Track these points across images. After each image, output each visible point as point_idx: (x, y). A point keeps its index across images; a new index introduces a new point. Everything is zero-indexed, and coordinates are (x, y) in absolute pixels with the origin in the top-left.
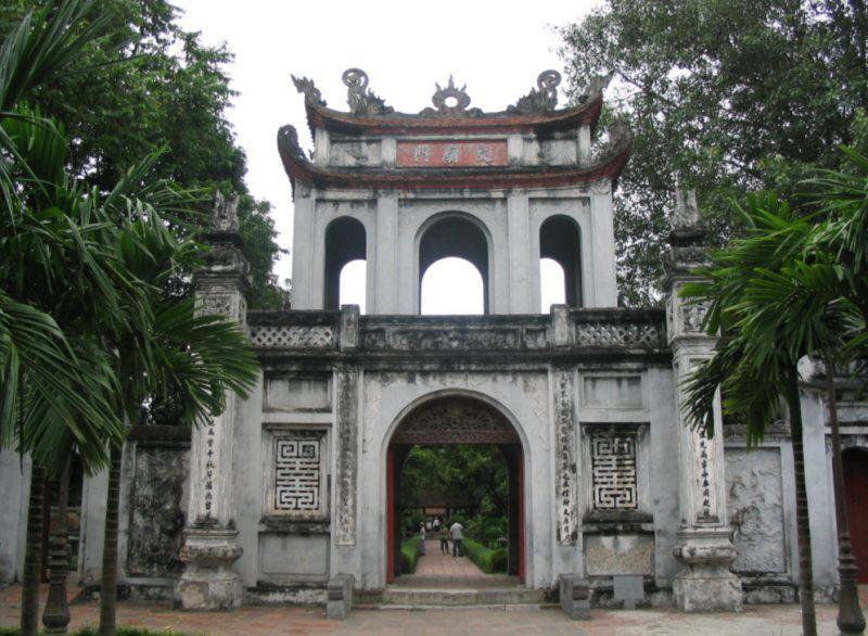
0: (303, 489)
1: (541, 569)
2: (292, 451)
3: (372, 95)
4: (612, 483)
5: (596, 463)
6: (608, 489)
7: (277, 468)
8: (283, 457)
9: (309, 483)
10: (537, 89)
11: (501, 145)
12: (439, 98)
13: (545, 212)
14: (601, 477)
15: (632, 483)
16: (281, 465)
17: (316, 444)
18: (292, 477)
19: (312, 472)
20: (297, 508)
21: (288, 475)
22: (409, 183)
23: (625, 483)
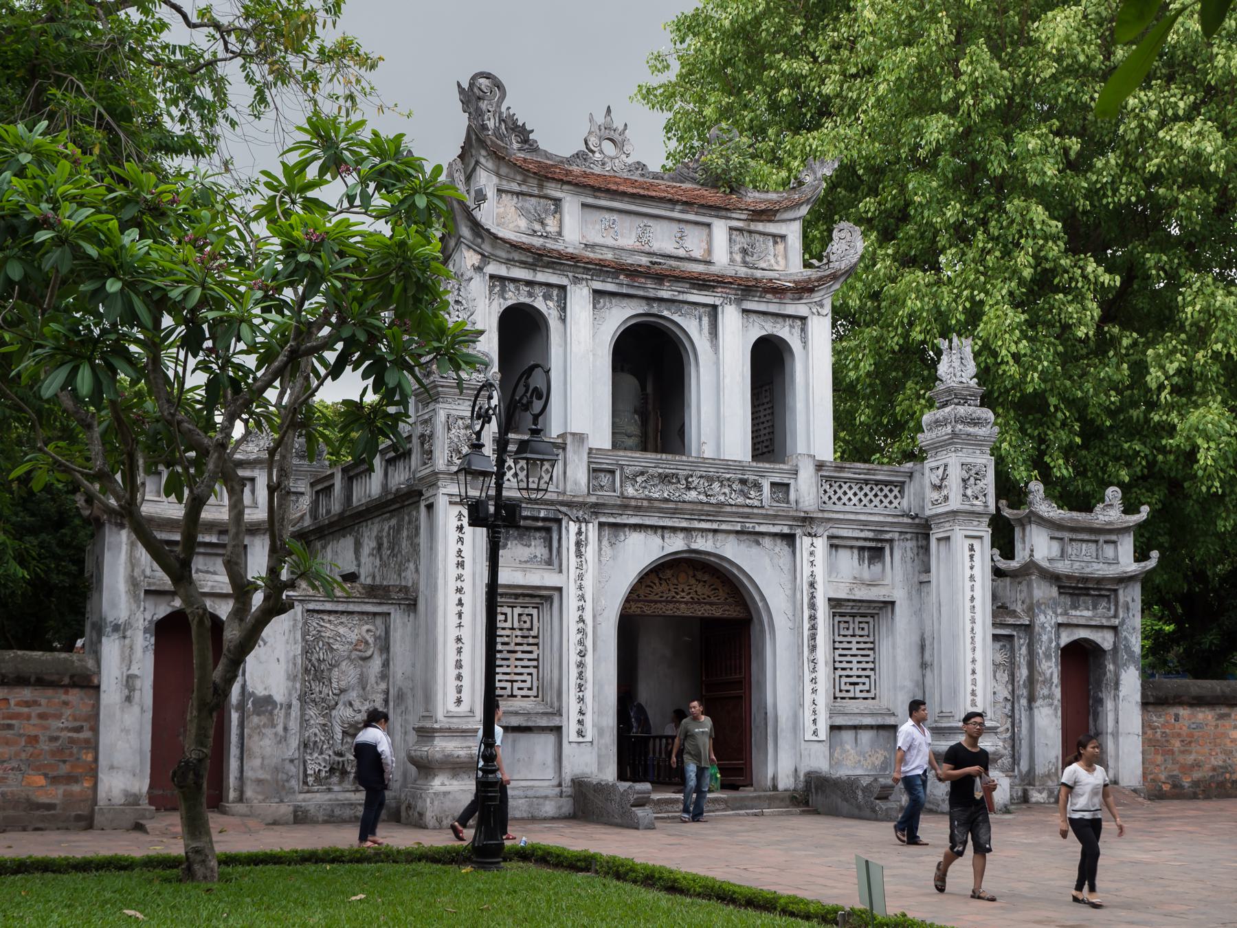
0: (519, 670)
2: (506, 621)
5: (837, 645)
6: (848, 676)
9: (526, 663)
11: (705, 231)
15: (872, 669)
19: (529, 648)
20: (513, 696)
22: (611, 274)
23: (864, 669)
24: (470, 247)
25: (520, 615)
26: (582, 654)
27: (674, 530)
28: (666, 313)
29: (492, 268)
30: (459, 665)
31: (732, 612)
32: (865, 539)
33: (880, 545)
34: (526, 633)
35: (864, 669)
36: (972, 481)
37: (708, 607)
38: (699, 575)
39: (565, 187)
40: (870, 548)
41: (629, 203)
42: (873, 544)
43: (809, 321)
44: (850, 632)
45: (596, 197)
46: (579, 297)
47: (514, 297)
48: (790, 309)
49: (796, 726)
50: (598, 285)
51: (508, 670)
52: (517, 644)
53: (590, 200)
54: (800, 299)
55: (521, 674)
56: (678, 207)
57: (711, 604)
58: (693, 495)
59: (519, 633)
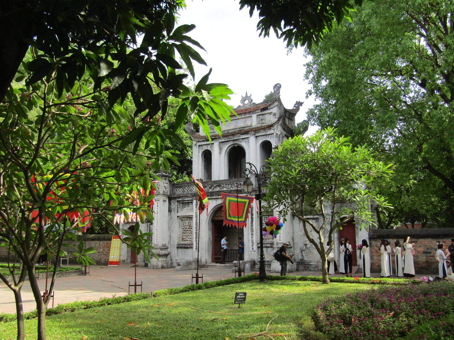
10: (273, 92)
12: (243, 100)
13: (261, 140)
27: (219, 198)
28: (237, 143)
29: (199, 144)
47: (205, 148)
49: (249, 248)
50: (221, 141)
56: (243, 115)
58: (225, 189)
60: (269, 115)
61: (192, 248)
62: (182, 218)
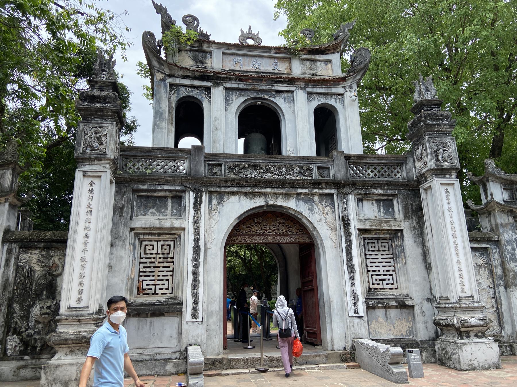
0: (161, 278)
1: (337, 331)
2: (153, 249)
3: (202, 32)
4: (379, 271)
5: (368, 257)
6: (377, 275)
7: (141, 263)
8: (145, 253)
14: (372, 267)
16: (142, 260)
17: (172, 244)
18: (152, 269)
19: (168, 265)
21: (149, 267)
23: (388, 271)
24: (159, 71)
25: (162, 246)
26: (196, 267)
28: (266, 97)
29: (170, 80)
30: (82, 276)
31: (302, 240)
32: (380, 195)
33: (390, 198)
34: (165, 256)
35: (388, 271)
36: (441, 150)
37: (285, 237)
38: (279, 220)
39: (213, 45)
40: (384, 200)
41: (246, 51)
42: (386, 198)
43: (345, 96)
44: (376, 248)
45: (229, 49)
46: (218, 93)
47: (183, 92)
48: (334, 90)
49: (343, 308)
51: (153, 278)
52: (159, 263)
53: (227, 51)
54: (339, 85)
55: (162, 280)
57: (287, 236)
59: (161, 256)
60: (323, 64)
61: (179, 313)
62: (140, 235)
